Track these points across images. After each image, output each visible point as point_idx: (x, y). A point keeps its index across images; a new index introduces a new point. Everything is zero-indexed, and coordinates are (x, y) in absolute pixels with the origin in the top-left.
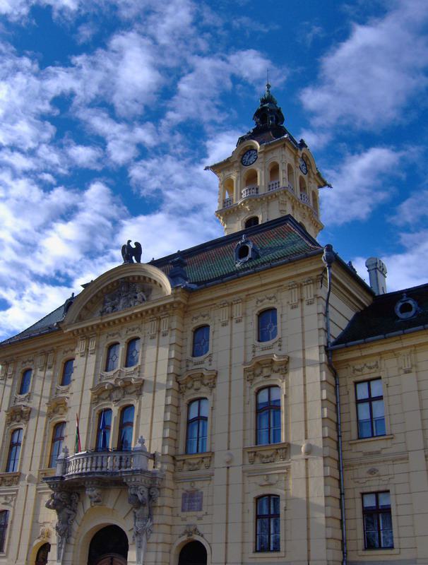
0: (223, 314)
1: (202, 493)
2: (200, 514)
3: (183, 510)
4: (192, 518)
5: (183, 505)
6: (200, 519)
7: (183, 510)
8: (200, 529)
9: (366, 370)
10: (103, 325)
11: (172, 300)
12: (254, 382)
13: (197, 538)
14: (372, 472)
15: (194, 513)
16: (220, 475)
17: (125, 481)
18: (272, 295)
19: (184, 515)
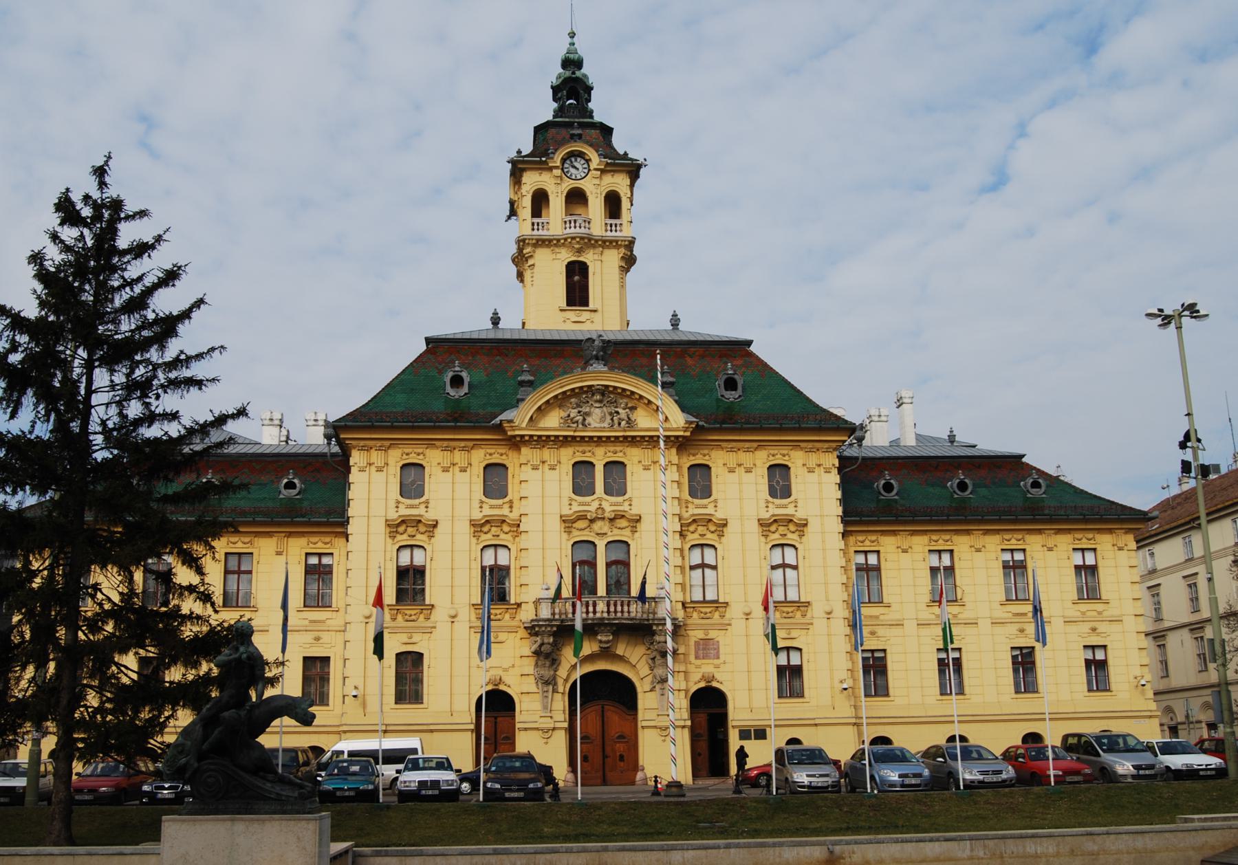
0: (732, 459)
1: (718, 642)
2: (716, 662)
3: (697, 658)
4: (707, 667)
5: (696, 652)
6: (717, 667)
7: (697, 658)
8: (717, 676)
9: (867, 543)
10: (574, 437)
11: (681, 433)
12: (769, 539)
13: (715, 684)
14: (873, 633)
15: (711, 661)
16: (738, 626)
17: (654, 628)
18: (785, 452)
19: (698, 662)
